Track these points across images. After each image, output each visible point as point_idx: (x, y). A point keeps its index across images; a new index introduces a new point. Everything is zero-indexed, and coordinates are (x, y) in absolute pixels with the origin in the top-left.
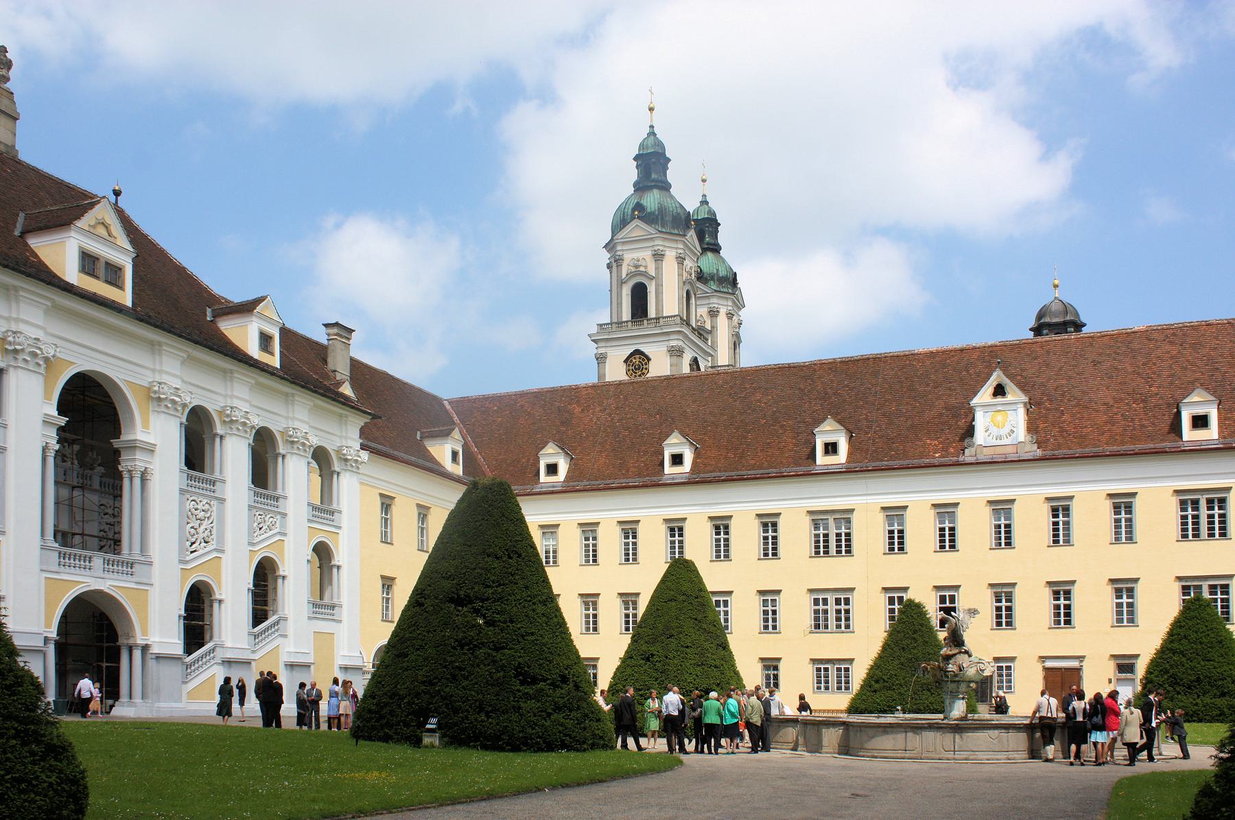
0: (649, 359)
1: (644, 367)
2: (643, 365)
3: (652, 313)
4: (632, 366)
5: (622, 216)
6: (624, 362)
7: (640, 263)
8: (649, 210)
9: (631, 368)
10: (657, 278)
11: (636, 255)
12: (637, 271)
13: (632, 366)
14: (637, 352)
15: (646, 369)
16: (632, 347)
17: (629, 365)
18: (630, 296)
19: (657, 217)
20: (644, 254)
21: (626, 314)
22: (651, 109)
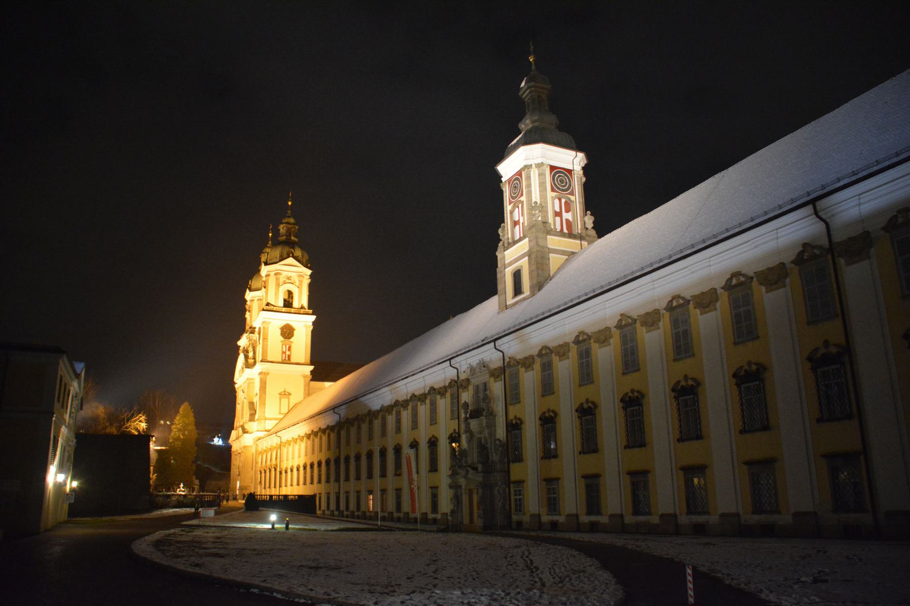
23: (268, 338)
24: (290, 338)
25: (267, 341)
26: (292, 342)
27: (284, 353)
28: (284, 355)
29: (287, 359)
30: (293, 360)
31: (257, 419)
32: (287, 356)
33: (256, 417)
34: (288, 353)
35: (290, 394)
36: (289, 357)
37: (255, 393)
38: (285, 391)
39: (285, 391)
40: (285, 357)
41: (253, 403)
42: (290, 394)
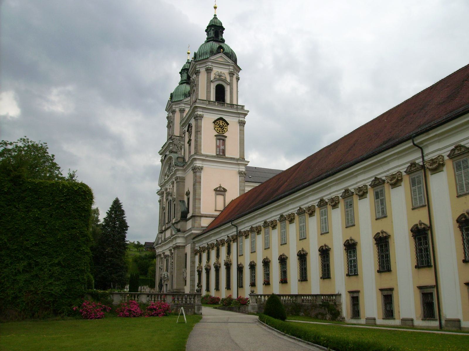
0: (228, 124)
1: (225, 127)
2: (224, 126)
3: (228, 100)
4: (218, 125)
5: (211, 49)
6: (213, 122)
7: (222, 75)
8: (226, 51)
9: (217, 126)
10: (230, 84)
11: (220, 70)
12: (220, 77)
13: (218, 125)
14: (221, 119)
15: (226, 129)
16: (218, 115)
17: (216, 125)
18: (215, 89)
19: (231, 56)
20: (225, 71)
21: (213, 98)
22: (215, 8)
23: (201, 130)
24: (224, 132)
25: (201, 134)
26: (226, 137)
27: (217, 147)
28: (218, 149)
29: (221, 154)
30: (227, 155)
31: (193, 217)
32: (221, 151)
33: (189, 216)
34: (222, 147)
35: (225, 190)
36: (224, 151)
37: (186, 190)
38: (220, 187)
39: (220, 187)
40: (220, 152)
41: (184, 202)
42: (225, 190)
